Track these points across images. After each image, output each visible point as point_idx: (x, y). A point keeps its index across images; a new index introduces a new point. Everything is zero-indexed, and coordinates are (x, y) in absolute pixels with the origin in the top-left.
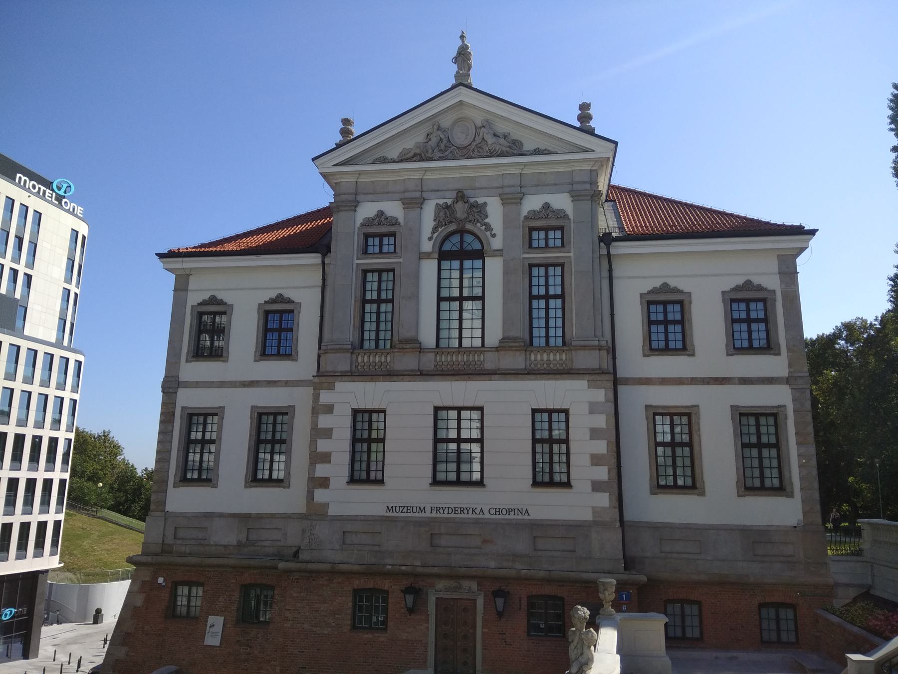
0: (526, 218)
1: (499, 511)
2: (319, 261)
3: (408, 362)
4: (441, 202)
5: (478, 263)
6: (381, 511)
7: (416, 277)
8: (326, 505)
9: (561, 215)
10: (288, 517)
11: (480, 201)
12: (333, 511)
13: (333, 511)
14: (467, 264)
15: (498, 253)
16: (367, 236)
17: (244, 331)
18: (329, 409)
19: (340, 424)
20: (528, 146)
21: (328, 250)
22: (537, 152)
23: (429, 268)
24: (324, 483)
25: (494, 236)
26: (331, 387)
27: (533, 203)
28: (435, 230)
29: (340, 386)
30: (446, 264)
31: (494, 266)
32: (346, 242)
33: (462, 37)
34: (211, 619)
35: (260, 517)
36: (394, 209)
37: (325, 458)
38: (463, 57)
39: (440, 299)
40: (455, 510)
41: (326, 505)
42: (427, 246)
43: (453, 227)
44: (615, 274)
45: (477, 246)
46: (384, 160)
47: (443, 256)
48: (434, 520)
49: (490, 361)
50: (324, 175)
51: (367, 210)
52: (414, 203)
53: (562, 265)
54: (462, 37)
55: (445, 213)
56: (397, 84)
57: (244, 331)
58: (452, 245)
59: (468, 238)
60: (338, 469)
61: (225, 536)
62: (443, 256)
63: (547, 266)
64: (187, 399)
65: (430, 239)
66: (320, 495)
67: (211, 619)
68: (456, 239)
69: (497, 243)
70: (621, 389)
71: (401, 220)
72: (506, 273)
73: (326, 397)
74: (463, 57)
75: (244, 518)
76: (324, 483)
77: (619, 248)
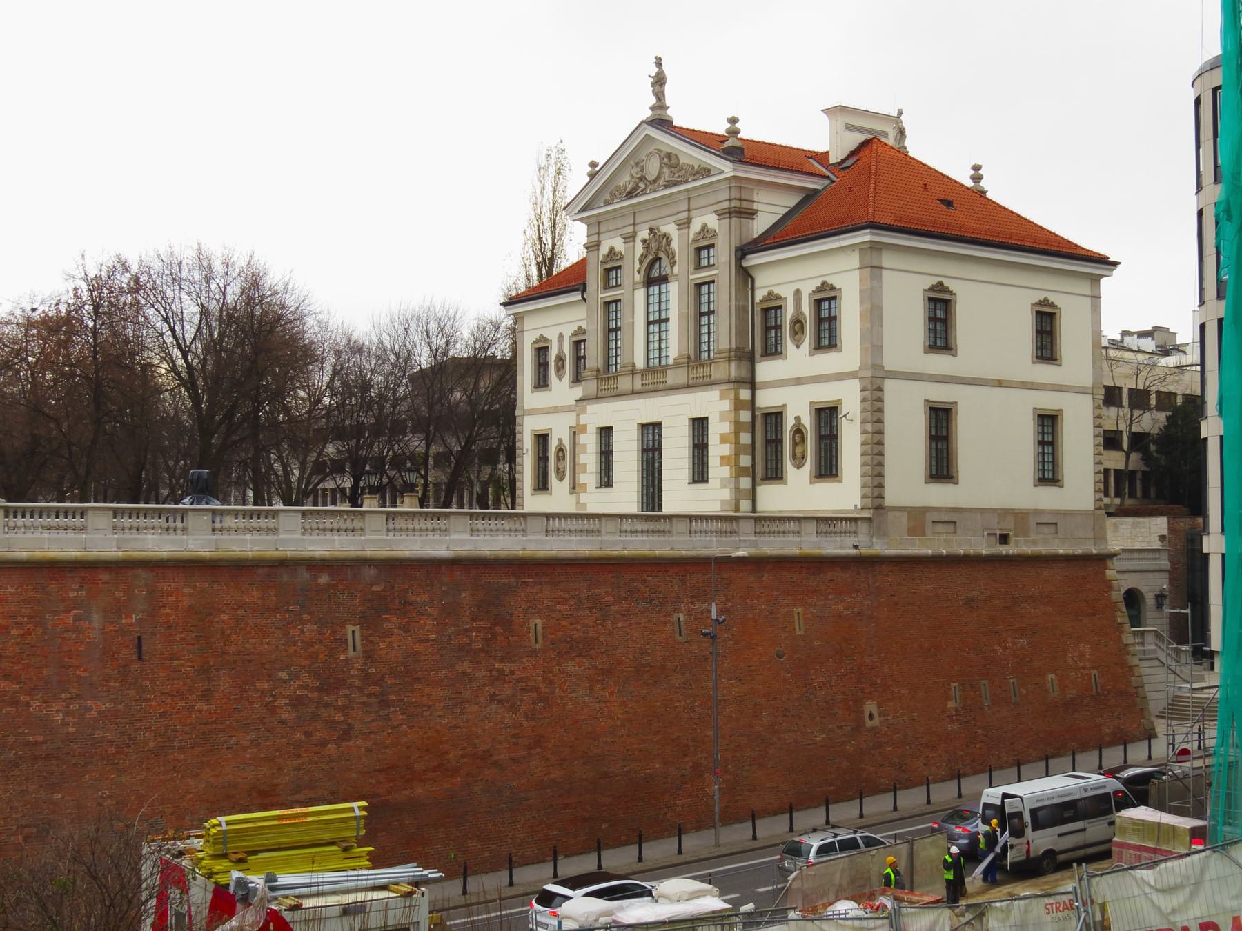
0: (695, 241)
2: (580, 298)
3: (624, 383)
14: (663, 286)
16: (608, 271)
21: (584, 290)
23: (640, 294)
27: (696, 226)
29: (592, 408)
30: (651, 289)
32: (594, 279)
33: (659, 62)
36: (619, 244)
38: (659, 81)
39: (649, 323)
42: (637, 277)
43: (650, 257)
44: (757, 284)
45: (668, 271)
47: (649, 282)
50: (581, 220)
54: (659, 62)
56: (601, 130)
58: (655, 274)
62: (649, 282)
63: (709, 283)
68: (657, 265)
70: (759, 393)
74: (659, 81)
77: (753, 260)
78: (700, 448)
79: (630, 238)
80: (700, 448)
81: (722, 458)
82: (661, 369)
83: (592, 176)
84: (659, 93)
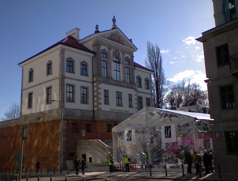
0: (126, 58)
1: (125, 111)
3: (111, 82)
4: (114, 50)
5: (119, 64)
6: (109, 110)
7: (111, 64)
8: (101, 108)
9: (129, 59)
10: (89, 111)
11: (120, 52)
12: (102, 109)
13: (102, 109)
15: (122, 64)
17: (78, 67)
18: (100, 89)
19: (102, 91)
20: (125, 44)
22: (127, 46)
23: (113, 64)
24: (100, 104)
25: (121, 60)
26: (100, 84)
27: (126, 55)
28: (113, 55)
31: (121, 65)
34: (82, 131)
35: (84, 110)
36: (107, 49)
37: (100, 99)
38: (114, 20)
40: (120, 111)
41: (101, 108)
43: (116, 56)
45: (118, 61)
46: (104, 37)
48: (117, 112)
49: (122, 84)
51: (102, 47)
52: (110, 49)
53: (129, 68)
55: (114, 53)
57: (78, 67)
59: (117, 59)
60: (102, 101)
61: (78, 114)
64: (67, 81)
65: (112, 57)
66: (100, 106)
67: (82, 131)
69: (122, 61)
71: (108, 52)
72: (123, 68)
73: (100, 86)
74: (114, 20)
75: (81, 110)
76: (100, 104)
78: (130, 100)
79: (110, 49)
80: (130, 100)
81: (136, 103)
82: (120, 81)
83: (97, 28)
84: (114, 23)
